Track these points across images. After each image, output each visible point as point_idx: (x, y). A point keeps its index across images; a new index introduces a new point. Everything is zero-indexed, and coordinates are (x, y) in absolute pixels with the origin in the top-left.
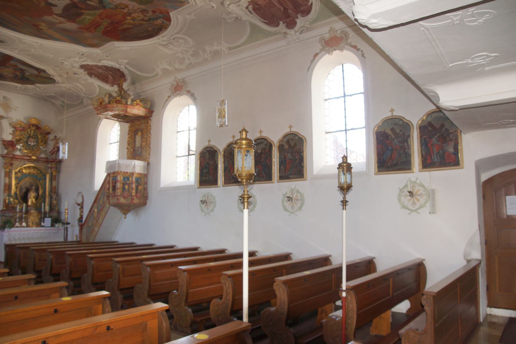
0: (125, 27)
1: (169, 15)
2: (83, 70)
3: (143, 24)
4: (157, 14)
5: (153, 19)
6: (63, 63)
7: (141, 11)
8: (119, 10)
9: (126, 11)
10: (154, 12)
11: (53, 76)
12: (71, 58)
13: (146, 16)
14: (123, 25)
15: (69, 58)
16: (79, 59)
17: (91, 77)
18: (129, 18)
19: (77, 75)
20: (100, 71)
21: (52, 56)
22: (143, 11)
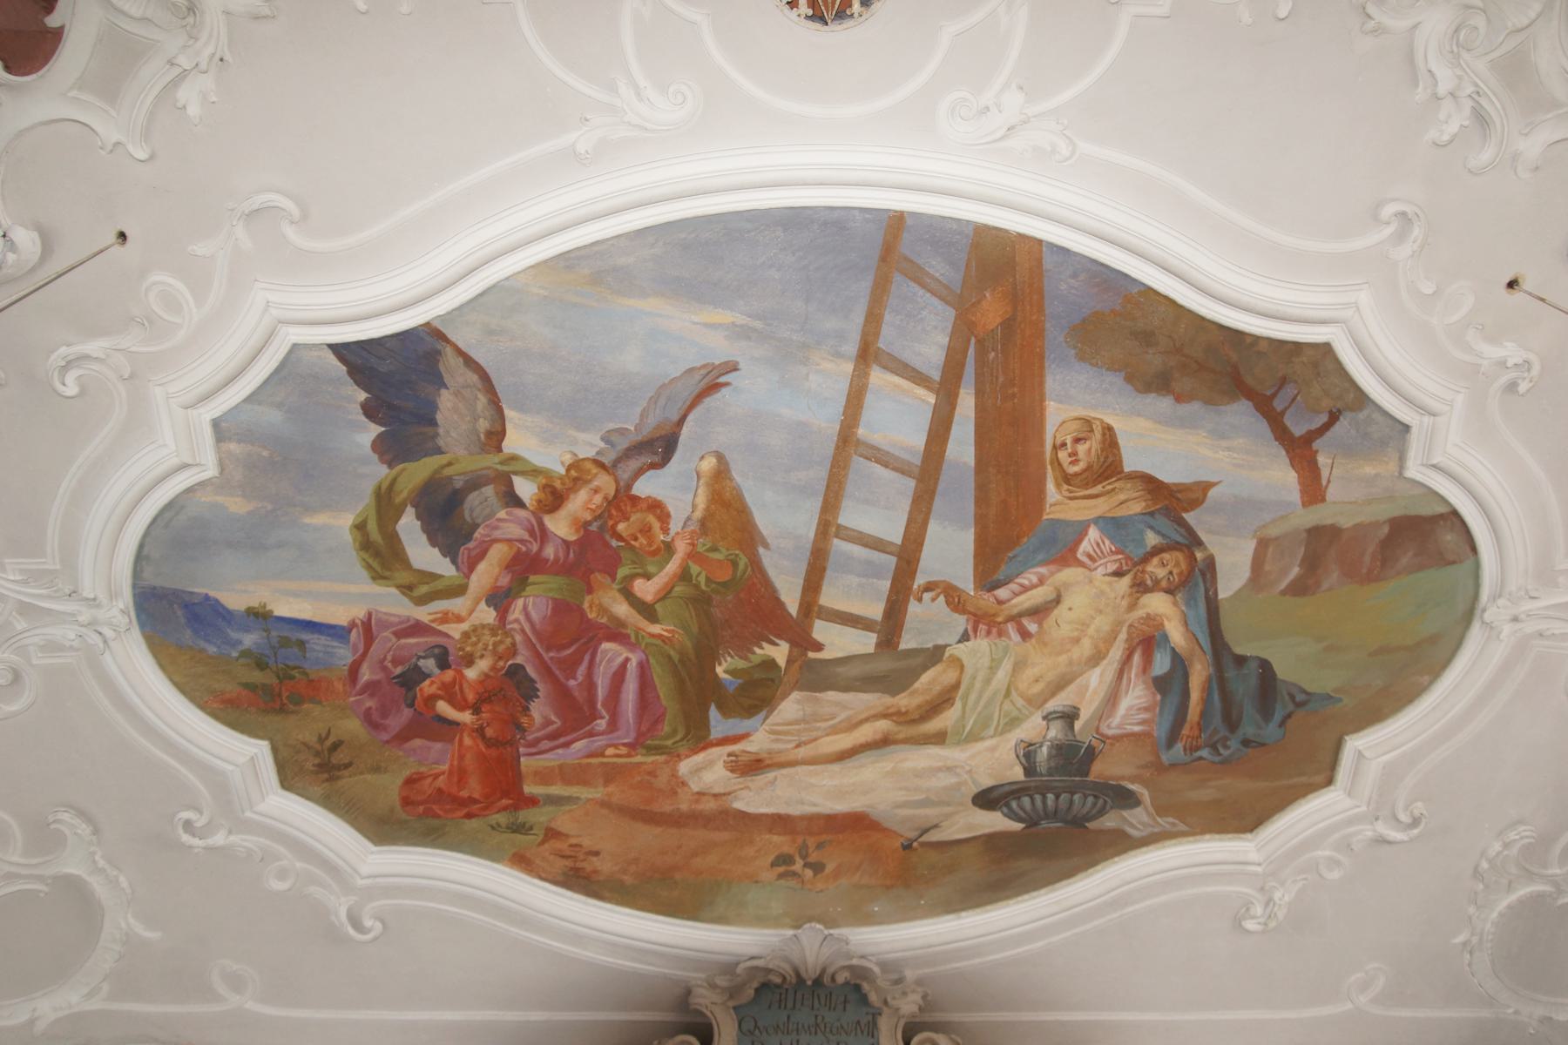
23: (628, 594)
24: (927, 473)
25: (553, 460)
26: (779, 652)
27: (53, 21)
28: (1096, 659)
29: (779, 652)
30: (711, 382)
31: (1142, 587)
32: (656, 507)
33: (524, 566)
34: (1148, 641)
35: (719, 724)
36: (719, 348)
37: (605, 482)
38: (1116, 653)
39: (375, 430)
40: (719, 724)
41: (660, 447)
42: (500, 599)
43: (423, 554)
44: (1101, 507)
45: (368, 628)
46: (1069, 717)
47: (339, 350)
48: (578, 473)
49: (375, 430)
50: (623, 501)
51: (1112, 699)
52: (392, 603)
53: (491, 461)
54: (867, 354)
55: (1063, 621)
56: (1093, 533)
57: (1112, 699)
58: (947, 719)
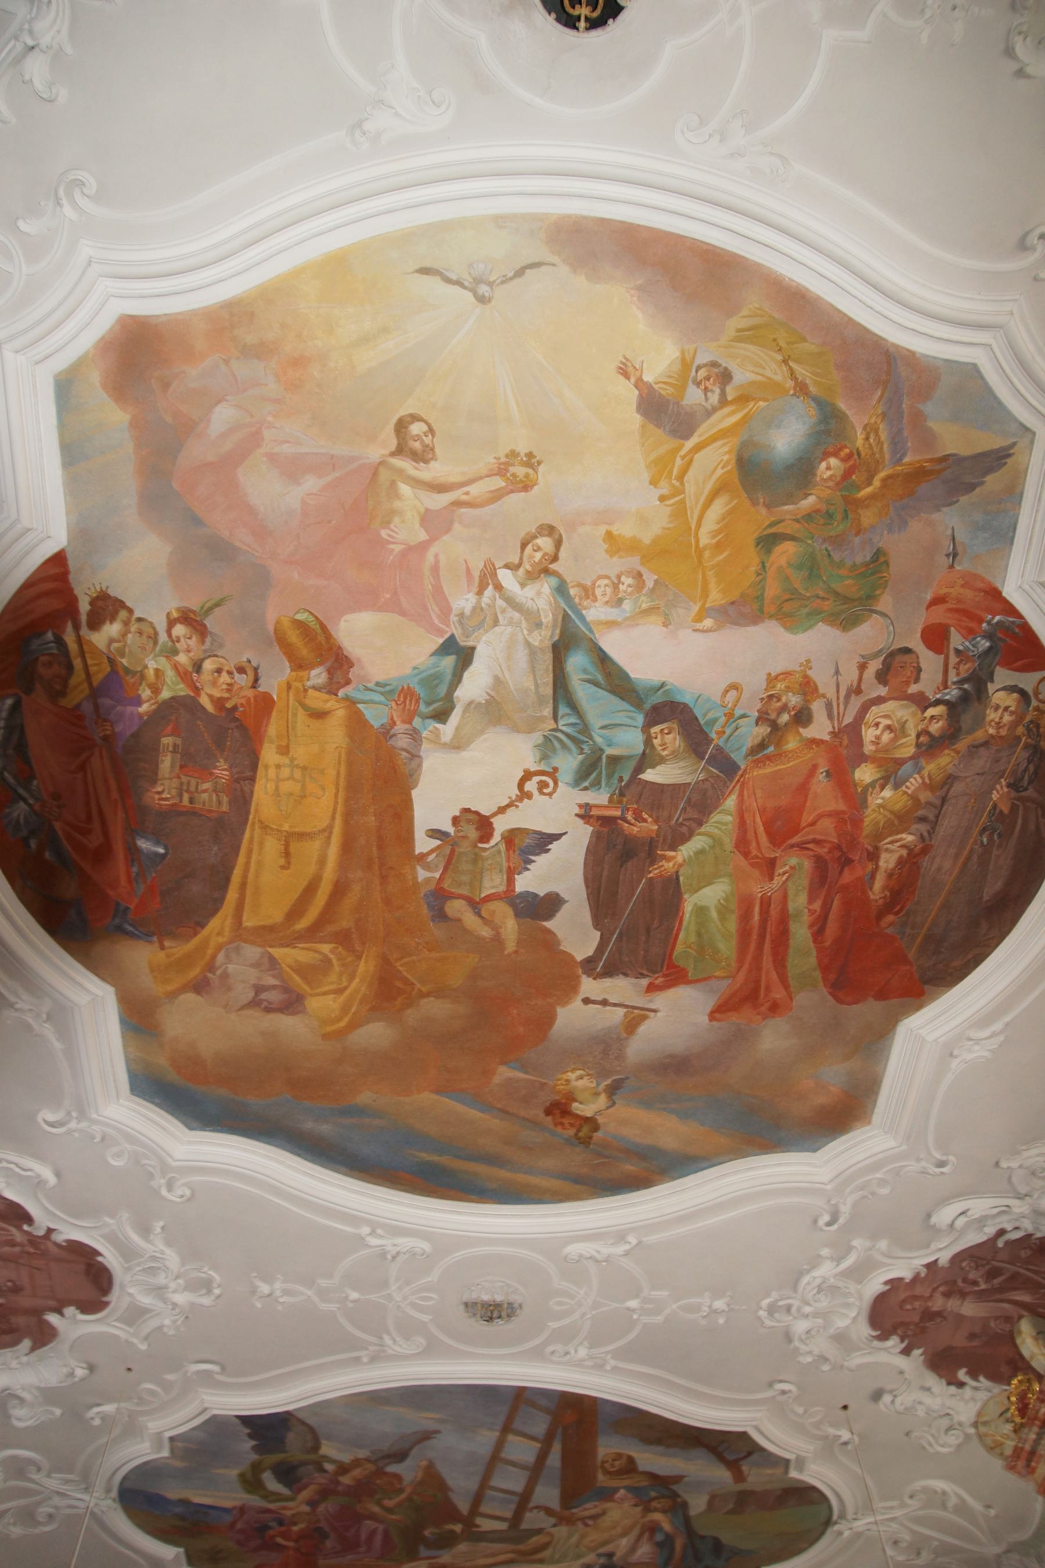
0: (887, 861)
1: (1011, 610)
2: (894, 1343)
3: (950, 779)
4: (956, 640)
5: (965, 698)
6: (788, 1337)
7: (882, 677)
8: (791, 744)
9: (820, 728)
10: (935, 638)
11: (801, 1463)
12: (801, 1274)
13: (922, 702)
14: (873, 856)
15: (795, 1288)
16: (839, 1260)
17: (961, 1385)
18: (865, 774)
19: (887, 1398)
20: (969, 1309)
21: (720, 1304)
22: (894, 666)
23: (379, 1503)
24: (536, 1470)
25: (346, 1458)
26: (458, 1528)
27: (105, 1299)
28: (624, 1534)
29: (458, 1528)
30: (426, 1436)
31: (647, 1510)
32: (397, 1477)
33: (325, 1493)
34: (653, 1529)
35: (423, 1552)
36: (431, 1426)
37: (371, 1467)
38: (635, 1533)
39: (253, 1443)
40: (423, 1552)
41: (401, 1456)
42: (313, 1503)
43: (272, 1484)
44: (627, 1482)
45: (242, 1510)
46: (610, 1555)
47: (238, 1417)
48: (357, 1463)
49: (253, 1443)
50: (380, 1473)
51: (633, 1549)
52: (255, 1501)
53: (312, 1457)
54: (507, 1429)
55: (606, 1521)
56: (622, 1492)
57: (633, 1549)
58: (546, 1553)
